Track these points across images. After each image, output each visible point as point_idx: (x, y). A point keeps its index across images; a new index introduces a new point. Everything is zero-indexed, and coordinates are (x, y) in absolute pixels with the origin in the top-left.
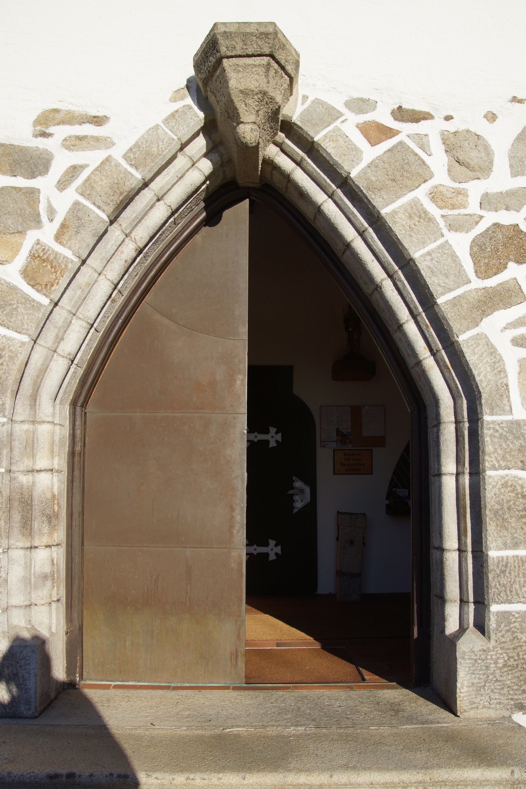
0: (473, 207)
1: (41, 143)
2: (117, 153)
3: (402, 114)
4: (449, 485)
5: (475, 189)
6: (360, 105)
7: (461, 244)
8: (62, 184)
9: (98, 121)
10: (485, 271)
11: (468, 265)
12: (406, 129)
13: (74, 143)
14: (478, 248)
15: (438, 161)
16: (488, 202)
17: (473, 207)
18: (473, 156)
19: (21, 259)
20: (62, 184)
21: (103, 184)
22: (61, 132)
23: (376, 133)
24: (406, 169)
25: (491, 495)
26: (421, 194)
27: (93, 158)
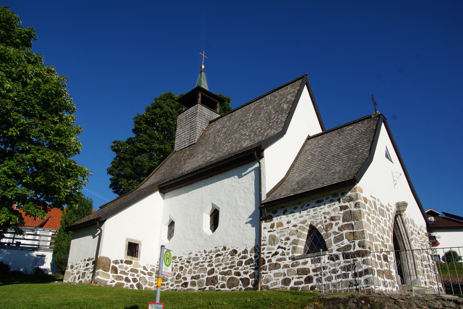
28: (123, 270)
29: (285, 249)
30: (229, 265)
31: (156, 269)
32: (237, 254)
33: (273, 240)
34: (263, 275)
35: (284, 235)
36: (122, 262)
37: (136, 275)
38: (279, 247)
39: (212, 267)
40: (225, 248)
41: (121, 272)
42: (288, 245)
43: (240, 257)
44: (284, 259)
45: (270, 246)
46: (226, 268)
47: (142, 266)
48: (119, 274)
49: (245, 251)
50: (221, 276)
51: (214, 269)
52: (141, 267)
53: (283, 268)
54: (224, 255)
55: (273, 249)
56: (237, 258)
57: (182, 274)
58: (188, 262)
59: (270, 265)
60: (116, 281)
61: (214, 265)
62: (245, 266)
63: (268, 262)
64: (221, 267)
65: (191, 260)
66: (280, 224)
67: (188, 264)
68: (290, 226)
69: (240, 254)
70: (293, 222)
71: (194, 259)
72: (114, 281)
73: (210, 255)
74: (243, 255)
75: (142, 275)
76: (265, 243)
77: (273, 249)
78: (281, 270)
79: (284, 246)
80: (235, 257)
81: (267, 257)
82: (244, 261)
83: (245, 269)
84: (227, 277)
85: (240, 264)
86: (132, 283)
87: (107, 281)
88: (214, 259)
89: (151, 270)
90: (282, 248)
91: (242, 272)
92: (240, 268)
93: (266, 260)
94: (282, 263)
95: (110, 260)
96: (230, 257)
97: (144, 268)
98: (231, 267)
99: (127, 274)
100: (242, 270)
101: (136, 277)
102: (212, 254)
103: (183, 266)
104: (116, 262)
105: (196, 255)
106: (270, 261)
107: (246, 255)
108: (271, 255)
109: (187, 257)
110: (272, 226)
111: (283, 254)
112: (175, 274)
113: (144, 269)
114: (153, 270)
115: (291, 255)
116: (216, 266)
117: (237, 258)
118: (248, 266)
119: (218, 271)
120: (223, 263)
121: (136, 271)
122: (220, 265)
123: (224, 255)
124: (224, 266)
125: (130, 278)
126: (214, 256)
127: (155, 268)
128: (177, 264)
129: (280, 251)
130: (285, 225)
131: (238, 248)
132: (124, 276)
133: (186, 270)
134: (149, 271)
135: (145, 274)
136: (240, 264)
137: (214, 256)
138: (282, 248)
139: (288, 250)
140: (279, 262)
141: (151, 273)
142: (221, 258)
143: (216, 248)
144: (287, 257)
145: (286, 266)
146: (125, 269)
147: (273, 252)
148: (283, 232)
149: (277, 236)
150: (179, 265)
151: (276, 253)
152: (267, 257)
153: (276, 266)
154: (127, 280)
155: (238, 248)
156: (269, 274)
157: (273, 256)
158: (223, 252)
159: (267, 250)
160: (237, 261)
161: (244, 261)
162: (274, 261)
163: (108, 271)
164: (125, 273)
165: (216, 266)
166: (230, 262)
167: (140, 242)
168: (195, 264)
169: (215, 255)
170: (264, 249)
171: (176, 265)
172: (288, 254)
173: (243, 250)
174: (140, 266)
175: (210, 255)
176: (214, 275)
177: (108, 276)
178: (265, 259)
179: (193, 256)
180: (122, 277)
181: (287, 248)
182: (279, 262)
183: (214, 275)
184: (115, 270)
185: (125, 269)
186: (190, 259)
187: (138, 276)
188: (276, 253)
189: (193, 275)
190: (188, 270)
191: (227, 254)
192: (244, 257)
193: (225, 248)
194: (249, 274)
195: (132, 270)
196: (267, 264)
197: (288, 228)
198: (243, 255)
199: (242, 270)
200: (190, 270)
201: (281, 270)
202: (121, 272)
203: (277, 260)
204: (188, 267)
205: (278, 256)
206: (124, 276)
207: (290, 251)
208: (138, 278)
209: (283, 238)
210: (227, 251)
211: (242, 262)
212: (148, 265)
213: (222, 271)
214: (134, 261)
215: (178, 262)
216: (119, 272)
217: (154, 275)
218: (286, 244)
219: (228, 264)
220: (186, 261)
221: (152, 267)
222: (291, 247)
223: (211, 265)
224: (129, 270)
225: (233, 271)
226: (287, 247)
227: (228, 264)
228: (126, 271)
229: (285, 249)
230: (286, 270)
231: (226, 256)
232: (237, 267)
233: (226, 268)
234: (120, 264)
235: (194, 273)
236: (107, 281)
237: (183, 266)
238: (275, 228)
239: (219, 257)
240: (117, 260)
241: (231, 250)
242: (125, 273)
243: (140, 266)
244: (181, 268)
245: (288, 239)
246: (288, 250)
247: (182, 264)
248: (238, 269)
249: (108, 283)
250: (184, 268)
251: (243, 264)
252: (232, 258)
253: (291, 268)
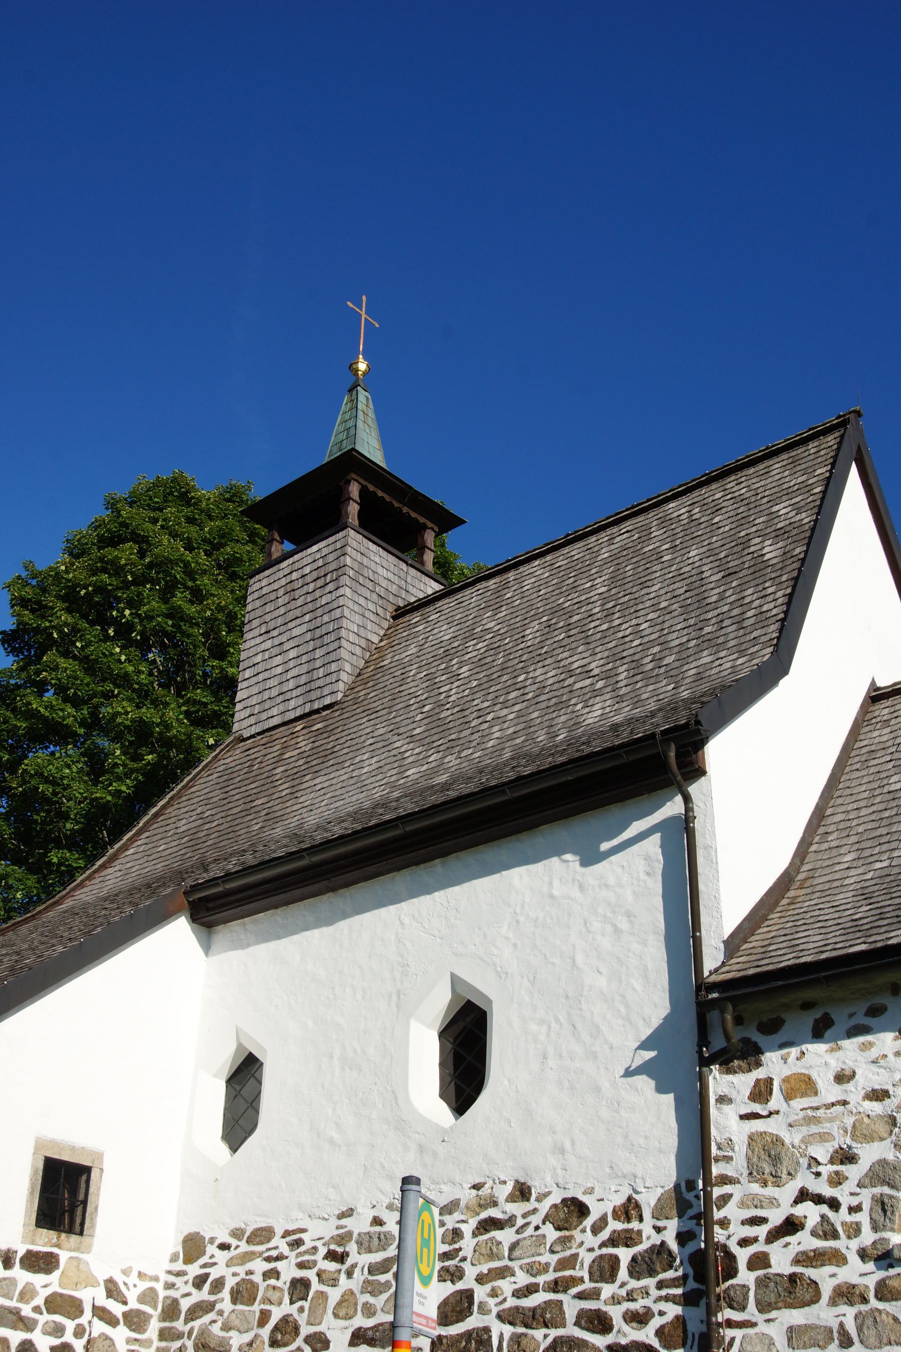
29: (834, 1204)
30: (550, 1276)
31: (162, 1294)
32: (588, 1222)
33: (769, 1159)
34: (729, 1333)
35: (824, 1137)
38: (803, 1196)
39: (460, 1286)
40: (522, 1192)
42: (850, 1186)
43: (605, 1235)
44: (838, 1258)
45: (756, 1188)
46: (530, 1290)
47: (102, 1277)
49: (629, 1209)
50: (508, 1330)
51: (468, 1295)
52: (94, 1283)
53: (833, 1302)
54: (520, 1222)
55: (773, 1202)
56: (587, 1244)
57: (302, 1319)
58: (332, 1256)
59: (759, 1282)
61: (471, 1272)
62: (634, 1284)
63: (751, 1266)
64: (506, 1286)
65: (352, 1248)
66: (802, 1085)
67: (332, 1266)
68: (854, 1092)
69: (602, 1222)
70: (869, 1077)
71: (366, 1244)
73: (451, 1221)
74: (619, 1226)
75: (99, 1327)
76: (728, 1170)
77: (773, 1202)
78: (823, 1314)
79: (828, 1191)
80: (576, 1233)
81: (744, 1242)
82: (625, 1255)
83: (630, 1297)
84: (538, 1333)
85: (606, 1269)
88: (468, 1244)
89: (142, 1299)
90: (818, 1199)
91: (616, 1313)
92: (607, 1290)
93: (743, 1255)
94: (826, 1278)
96: (551, 1233)
97: (112, 1290)
98: (556, 1286)
100: (615, 1300)
102: (457, 1216)
103: (311, 1274)
105: (377, 1222)
106: (759, 1261)
107: (634, 1225)
108: (761, 1231)
109: (329, 1230)
110: (762, 1092)
111: (828, 1231)
112: (264, 1317)
113: (110, 1294)
114: (148, 1297)
115: (867, 1237)
116: (481, 1279)
117: (587, 1244)
118: (650, 1282)
119: (492, 1302)
120: (515, 1265)
122: (503, 1273)
123: (520, 1222)
124: (522, 1279)
126: (467, 1229)
127: (159, 1287)
128: (279, 1265)
129: (811, 1213)
130: (829, 1092)
131: (590, 1191)
133: (322, 1295)
134: (133, 1304)
135: (112, 1321)
136: (606, 1269)
137: (467, 1229)
138: (818, 1199)
139: (853, 1210)
140: (811, 1273)
141: (138, 1313)
142: (506, 1237)
143: (477, 1187)
144: (849, 1247)
145: (847, 1294)
147: (776, 1218)
148: (816, 1120)
149: (791, 1138)
150: (288, 1271)
151: (791, 1226)
152: (744, 1242)
153: (794, 1290)
155: (590, 1191)
156: (762, 1328)
157: (774, 1236)
158: (517, 1209)
159: (743, 1205)
160: (587, 1258)
161: (625, 1255)
162: (781, 1260)
165: (481, 1279)
166: (553, 1259)
168: (373, 1269)
169: (473, 1223)
170: (725, 1199)
171: (274, 1274)
172: (855, 1230)
173: (619, 1200)
174: (91, 1282)
175: (451, 1221)
176: (473, 1322)
178: (735, 1249)
179: (360, 1225)
181: (846, 1201)
182: (811, 1273)
183: (473, 1322)
186: (343, 1238)
188: (791, 1226)
189: (360, 1321)
190: (334, 1295)
191: (536, 1219)
192: (627, 1239)
193: (522, 1192)
194: (656, 1322)
196: (746, 1277)
197: (845, 1103)
198: (619, 1226)
199: (615, 1300)
200: (348, 1298)
201: (823, 1314)
203: (797, 1261)
204: (334, 1283)
205: (804, 1241)
207: (863, 1218)
209: (822, 1153)
210: (533, 1204)
211: (615, 1262)
212: (126, 1272)
213: (511, 1302)
214: (64, 1256)
215: (279, 1258)
217: (154, 1326)
218: (837, 1180)
219: (545, 1268)
220: (323, 1251)
221: (144, 1285)
222: (866, 1198)
223: (455, 1275)
225: (571, 1307)
226: (842, 1194)
227: (545, 1268)
229: (834, 1204)
230: (848, 1314)
231: (530, 1231)
232: (588, 1285)
233: (530, 1290)
235: (369, 1311)
237: (311, 1274)
238: (776, 1100)
239: (497, 1234)
241: (556, 1198)
243: (91, 1282)
244: (299, 1287)
245: (846, 1157)
246: (853, 1210)
247: (301, 1266)
248: (594, 1295)
250: (315, 1286)
251: (623, 1273)
252: (564, 1241)
253: (874, 1303)
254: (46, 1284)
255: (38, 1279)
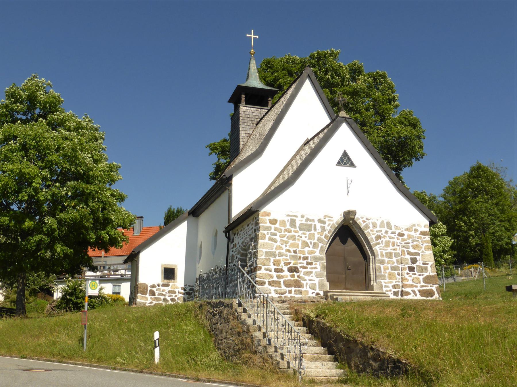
0: (375, 232)
1: (324, 220)
2: (334, 222)
3: (367, 219)
4: (371, 267)
5: (375, 230)
6: (362, 218)
7: (374, 237)
8: (328, 226)
9: (332, 217)
10: (376, 240)
11: (374, 240)
12: (367, 221)
13: (329, 220)
14: (376, 237)
15: (371, 226)
16: (377, 232)
17: (375, 232)
18: (375, 225)
19: (324, 235)
20: (328, 226)
21: (333, 226)
22: (327, 219)
23: (364, 222)
24: (367, 227)
25: (376, 267)
26: (369, 230)
27: (331, 223)
28: (161, 292)
36: (159, 285)
37: (174, 295)
41: (159, 294)
48: (157, 296)
60: (154, 302)
72: (152, 303)
86: (170, 302)
87: (146, 303)
89: (190, 290)
95: (147, 286)
99: (164, 295)
101: (173, 297)
104: (153, 286)
121: (174, 292)
125: (169, 298)
132: (162, 297)
146: (163, 291)
154: (165, 300)
163: (146, 294)
164: (162, 295)
167: (176, 266)
174: (177, 288)
177: (147, 299)
180: (160, 298)
184: (153, 293)
185: (163, 291)
187: (176, 296)
195: (169, 292)
202: (159, 294)
206: (162, 297)
208: (176, 298)
214: (171, 284)
216: (156, 294)
224: (167, 291)
228: (164, 293)
234: (157, 287)
236: (146, 303)
240: (154, 285)
242: (162, 295)
243: (177, 288)
249: (147, 305)
254: (167, 289)
255: (166, 288)
